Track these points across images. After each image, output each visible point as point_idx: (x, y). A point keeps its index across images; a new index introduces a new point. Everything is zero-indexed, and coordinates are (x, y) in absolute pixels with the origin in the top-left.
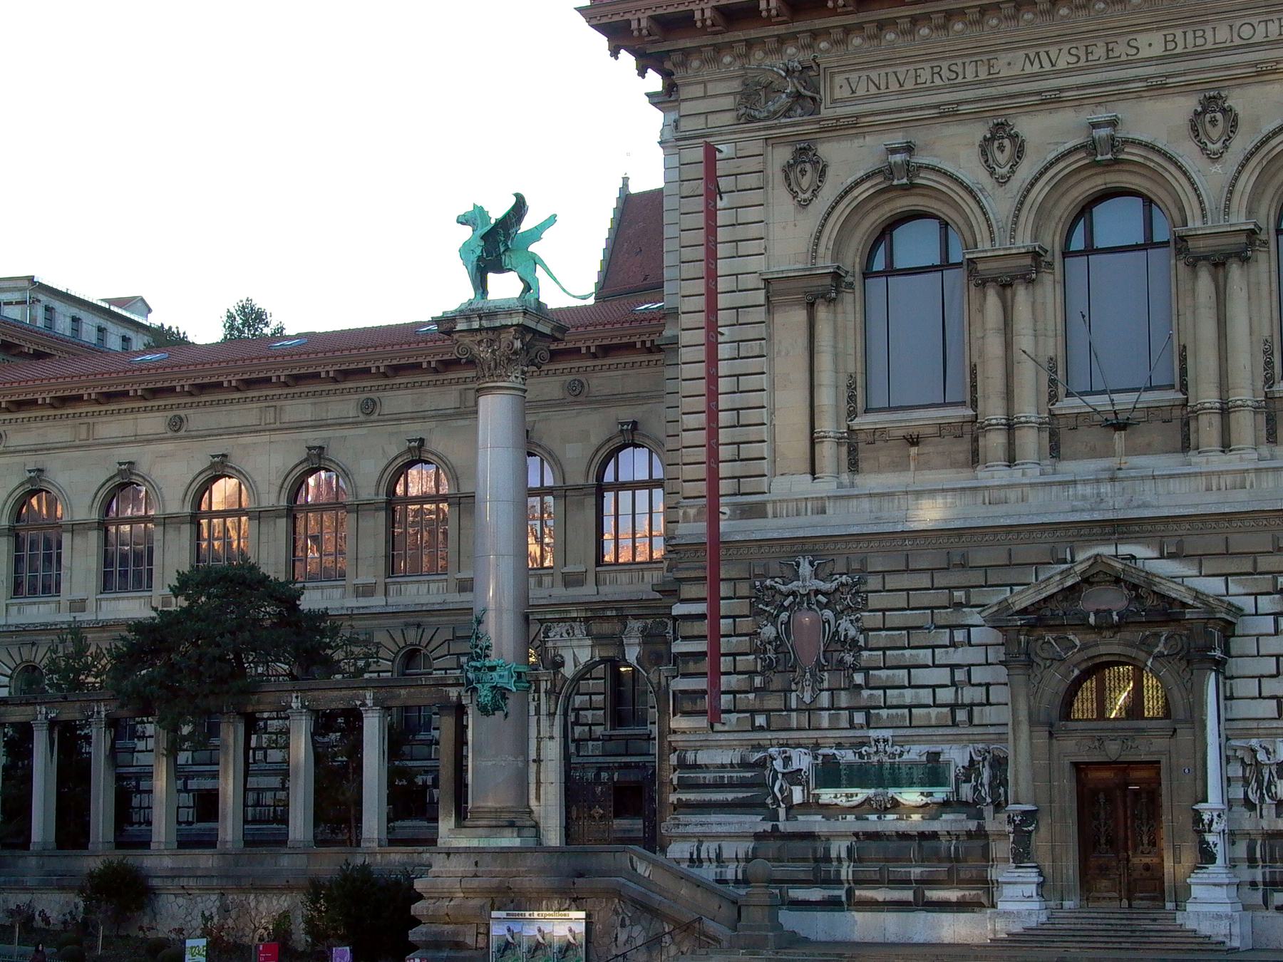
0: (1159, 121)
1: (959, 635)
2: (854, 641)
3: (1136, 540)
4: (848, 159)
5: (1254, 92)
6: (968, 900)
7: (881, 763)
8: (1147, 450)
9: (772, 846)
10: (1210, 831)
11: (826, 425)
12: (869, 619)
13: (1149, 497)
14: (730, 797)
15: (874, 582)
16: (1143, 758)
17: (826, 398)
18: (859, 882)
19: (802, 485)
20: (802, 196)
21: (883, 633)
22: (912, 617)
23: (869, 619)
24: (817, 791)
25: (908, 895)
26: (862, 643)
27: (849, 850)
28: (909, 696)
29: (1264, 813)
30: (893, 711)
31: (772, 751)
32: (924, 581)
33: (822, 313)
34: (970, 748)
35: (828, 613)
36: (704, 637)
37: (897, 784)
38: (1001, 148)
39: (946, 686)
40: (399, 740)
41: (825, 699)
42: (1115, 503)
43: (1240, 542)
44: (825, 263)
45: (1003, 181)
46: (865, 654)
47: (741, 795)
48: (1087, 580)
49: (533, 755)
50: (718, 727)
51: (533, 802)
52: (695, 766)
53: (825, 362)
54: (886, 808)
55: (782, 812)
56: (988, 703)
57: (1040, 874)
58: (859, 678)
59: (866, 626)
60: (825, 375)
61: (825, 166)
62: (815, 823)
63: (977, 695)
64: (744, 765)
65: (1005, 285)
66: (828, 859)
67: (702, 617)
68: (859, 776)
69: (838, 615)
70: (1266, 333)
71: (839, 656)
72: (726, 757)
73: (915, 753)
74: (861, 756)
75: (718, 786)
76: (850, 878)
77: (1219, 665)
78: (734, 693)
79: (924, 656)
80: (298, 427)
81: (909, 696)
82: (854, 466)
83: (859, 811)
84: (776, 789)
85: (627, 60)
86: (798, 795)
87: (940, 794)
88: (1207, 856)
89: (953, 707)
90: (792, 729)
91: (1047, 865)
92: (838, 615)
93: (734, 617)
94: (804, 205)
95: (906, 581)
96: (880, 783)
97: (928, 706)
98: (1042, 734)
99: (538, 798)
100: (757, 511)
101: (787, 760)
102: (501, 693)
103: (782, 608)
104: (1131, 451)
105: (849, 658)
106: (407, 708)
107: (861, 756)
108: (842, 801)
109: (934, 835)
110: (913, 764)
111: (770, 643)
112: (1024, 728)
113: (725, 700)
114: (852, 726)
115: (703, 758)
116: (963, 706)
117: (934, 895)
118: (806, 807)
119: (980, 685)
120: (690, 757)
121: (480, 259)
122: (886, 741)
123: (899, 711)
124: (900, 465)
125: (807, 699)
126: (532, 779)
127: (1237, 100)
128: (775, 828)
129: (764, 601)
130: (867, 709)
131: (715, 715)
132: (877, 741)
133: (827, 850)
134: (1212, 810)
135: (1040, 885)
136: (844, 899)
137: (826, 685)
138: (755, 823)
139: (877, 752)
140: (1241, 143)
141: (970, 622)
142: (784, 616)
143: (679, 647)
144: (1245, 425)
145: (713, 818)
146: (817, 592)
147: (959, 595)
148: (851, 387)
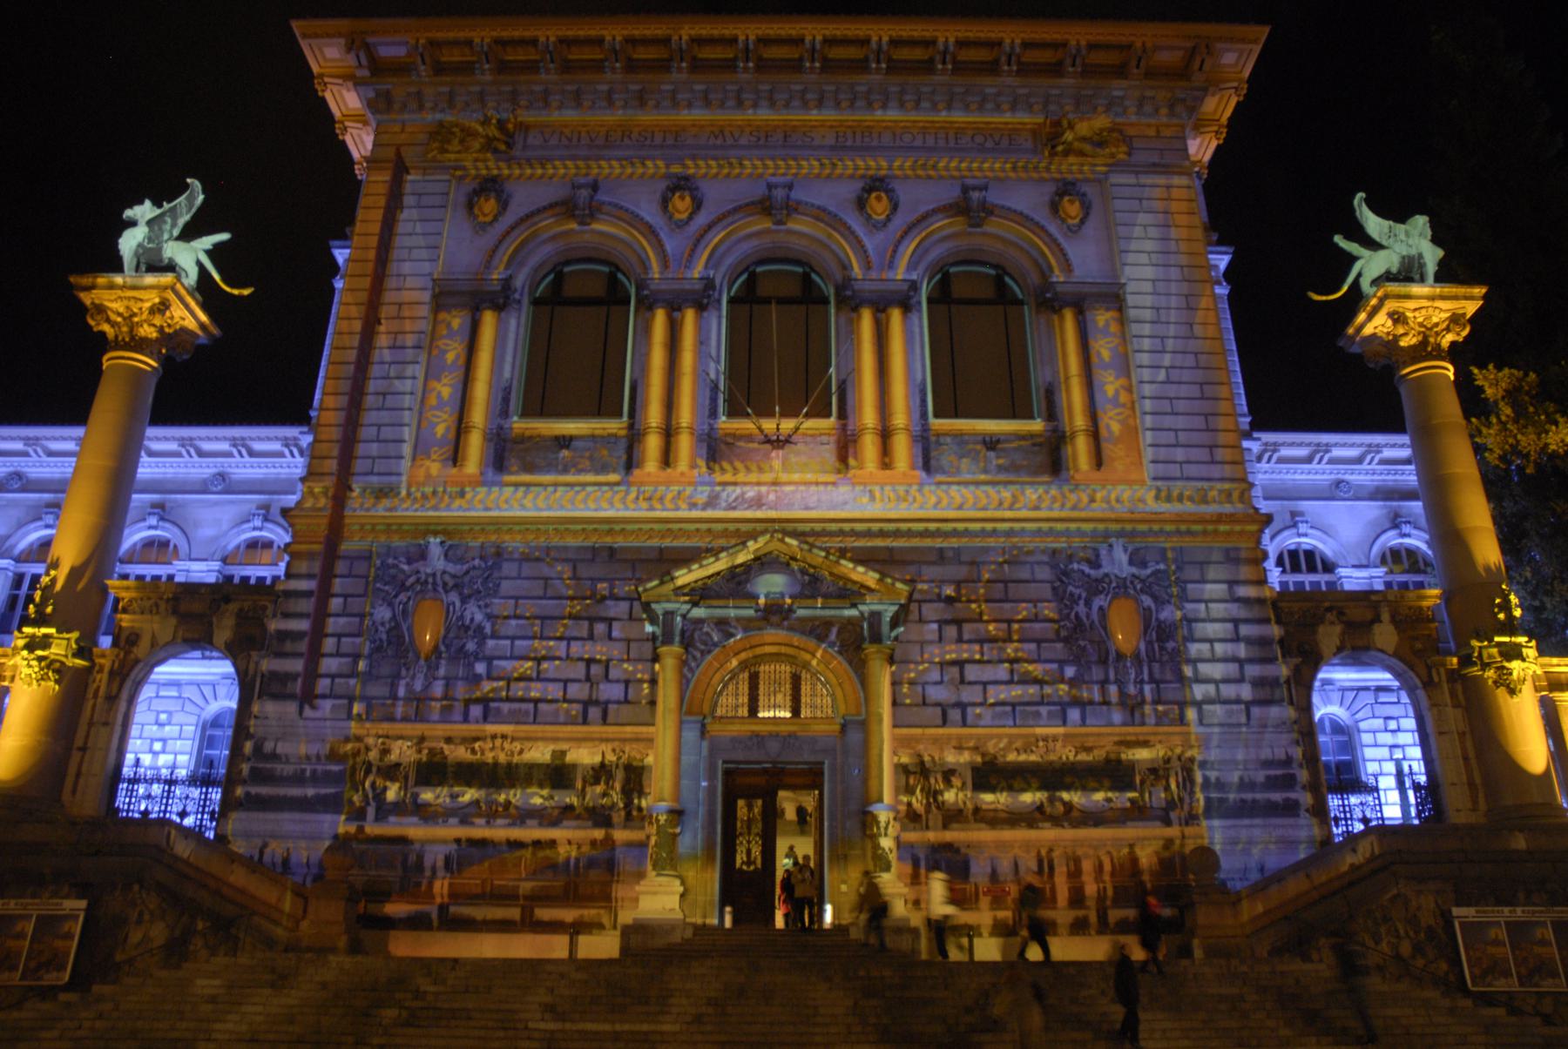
1: (600, 628)
2: (480, 628)
6: (586, 919)
11: (478, 416)
12: (500, 606)
13: (812, 501)
14: (310, 792)
15: (509, 568)
16: (807, 757)
20: (481, 219)
21: (513, 622)
23: (500, 606)
24: (416, 790)
25: (514, 913)
26: (488, 630)
27: (448, 859)
30: (516, 706)
31: (371, 741)
33: (489, 319)
34: (603, 747)
36: (306, 616)
38: (682, 198)
39: (579, 681)
41: (438, 689)
45: (682, 225)
46: (491, 643)
47: (323, 791)
49: (79, 742)
50: (308, 712)
51: (66, 796)
52: (274, 756)
55: (371, 812)
56: (627, 701)
57: (683, 883)
58: (480, 668)
59: (496, 612)
61: (510, 196)
63: (616, 691)
64: (333, 756)
66: (419, 866)
67: (307, 594)
68: (470, 774)
69: (464, 601)
70: (919, 377)
71: (460, 645)
74: (474, 751)
75: (299, 779)
76: (446, 891)
78: (333, 677)
83: (465, 815)
84: (367, 784)
86: (392, 794)
89: (587, 704)
92: (464, 601)
93: (346, 596)
94: (483, 227)
99: (74, 792)
101: (385, 751)
103: (403, 587)
104: (786, 467)
105: (471, 646)
107: (474, 751)
109: (553, 843)
110: (532, 767)
111: (383, 624)
113: (323, 685)
114: (466, 720)
115: (281, 749)
116: (596, 703)
117: (544, 914)
118: (399, 808)
119: (618, 681)
120: (268, 746)
121: (140, 245)
122: (504, 737)
123: (524, 706)
125: (418, 686)
126: (72, 770)
128: (361, 829)
130: (484, 701)
131: (308, 698)
132: (494, 737)
133: (420, 857)
135: (682, 896)
136: (434, 916)
139: (492, 749)
141: (611, 614)
142: (403, 597)
143: (274, 625)
145: (286, 816)
147: (602, 587)
148: (507, 391)
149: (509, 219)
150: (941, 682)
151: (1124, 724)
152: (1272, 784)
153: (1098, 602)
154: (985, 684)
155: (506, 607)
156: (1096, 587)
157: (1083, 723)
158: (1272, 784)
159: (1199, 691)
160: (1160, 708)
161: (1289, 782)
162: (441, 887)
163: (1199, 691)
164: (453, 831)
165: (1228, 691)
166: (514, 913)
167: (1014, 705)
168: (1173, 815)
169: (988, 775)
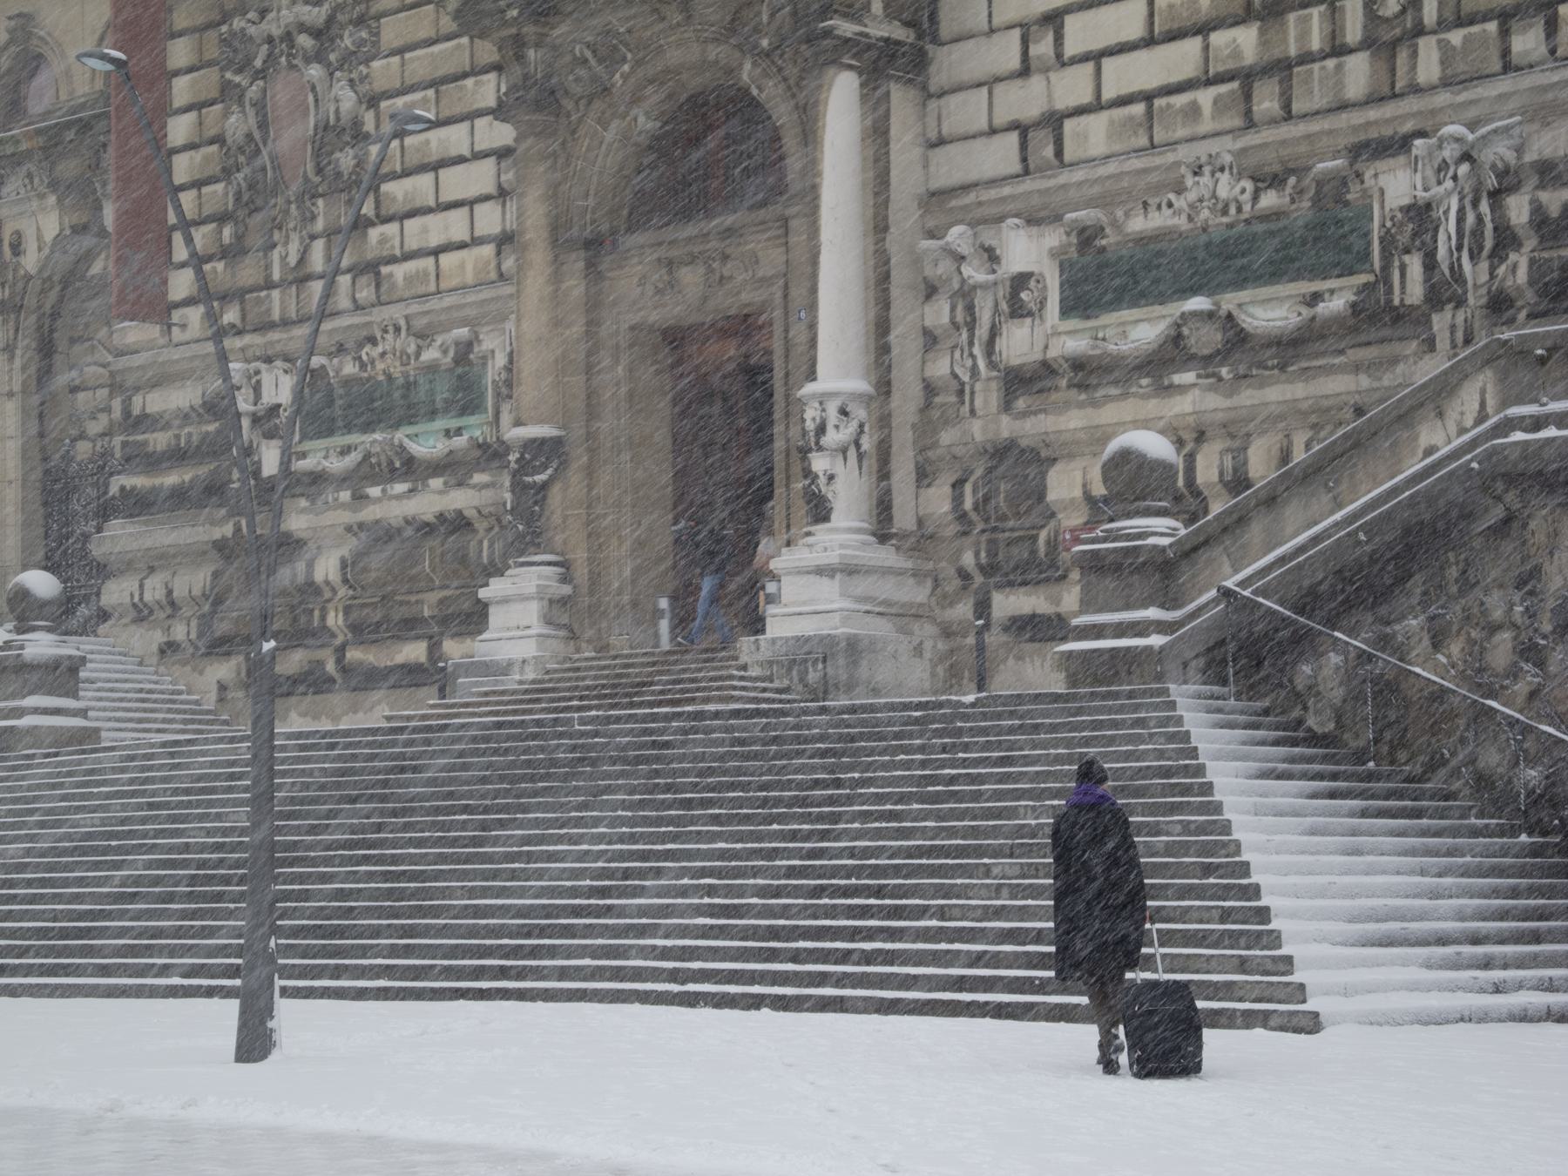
7: (389, 377)
10: (820, 448)
12: (383, 71)
18: (360, 631)
28: (437, 228)
29: (978, 402)
35: (315, 72)
54: (393, 470)
59: (379, 85)
75: (178, 456)
79: (455, 138)
81: (437, 228)
86: (270, 459)
88: (820, 511)
90: (272, 326)
91: (580, 556)
97: (462, 246)
98: (576, 263)
105: (345, 160)
106: (1340, 571)
108: (336, 465)
112: (539, 256)
134: (822, 399)
137: (320, 225)
146: (302, 28)
150: (1025, 71)
151: (1374, 99)
154: (1095, 58)
157: (1288, 115)
160: (1456, 37)
167: (1148, 97)
168: (1440, 322)
169: (1098, 280)
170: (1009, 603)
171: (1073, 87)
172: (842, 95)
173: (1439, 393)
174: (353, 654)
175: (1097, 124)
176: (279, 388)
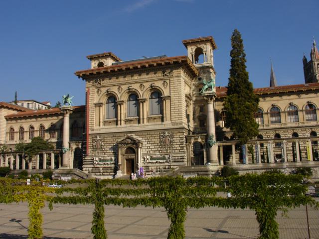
0: (136, 87)
3: (134, 133)
4: (104, 90)
5: (146, 83)
8: (135, 123)
9: (95, 169)
11: (101, 121)
17: (101, 118)
19: (98, 127)
22: (109, 142)
25: (108, 174)
32: (111, 138)
37: (107, 161)
40: (56, 157)
42: (131, 129)
43: (144, 134)
44: (101, 102)
48: (126, 138)
53: (101, 113)
60: (101, 115)
62: (98, 166)
65: (120, 105)
72: (90, 158)
73: (109, 158)
75: (88, 162)
77: (141, 148)
80: (50, 120)
82: (104, 125)
85: (81, 79)
87: (112, 162)
95: (109, 138)
96: (106, 161)
100: (93, 130)
102: (66, 151)
104: (133, 123)
105: (102, 147)
117: (111, 174)
124: (109, 125)
127: (145, 84)
129: (93, 141)
138: (92, 166)
140: (145, 89)
144: (145, 121)
149: (102, 94)
152: (181, 159)
153: (164, 139)
155: (105, 143)
156: (163, 137)
158: (181, 159)
159: (174, 148)
161: (183, 159)
162: (102, 171)
163: (174, 148)
164: (102, 166)
165: (177, 148)
166: (108, 174)
169: (152, 159)
170: (147, 173)
171: (150, 150)
172: (139, 149)
173: (176, 168)
174: (104, 174)
175: (151, 152)
176: (97, 159)
